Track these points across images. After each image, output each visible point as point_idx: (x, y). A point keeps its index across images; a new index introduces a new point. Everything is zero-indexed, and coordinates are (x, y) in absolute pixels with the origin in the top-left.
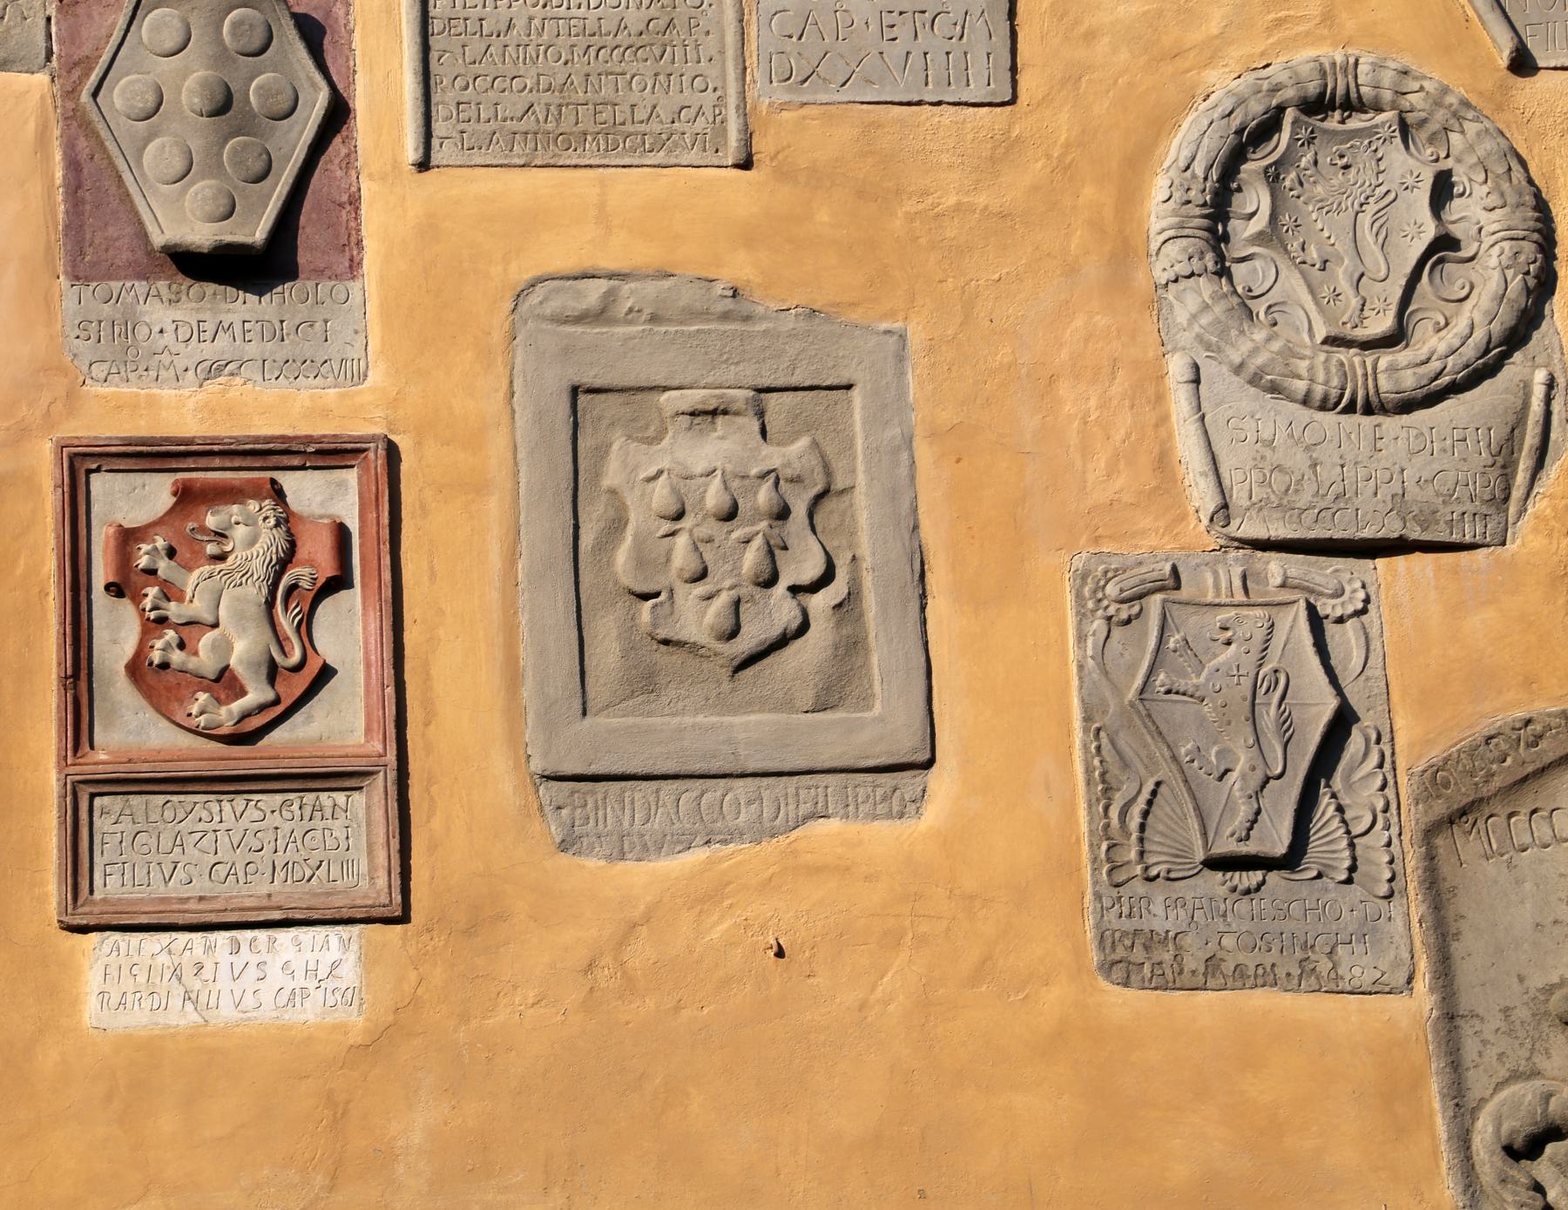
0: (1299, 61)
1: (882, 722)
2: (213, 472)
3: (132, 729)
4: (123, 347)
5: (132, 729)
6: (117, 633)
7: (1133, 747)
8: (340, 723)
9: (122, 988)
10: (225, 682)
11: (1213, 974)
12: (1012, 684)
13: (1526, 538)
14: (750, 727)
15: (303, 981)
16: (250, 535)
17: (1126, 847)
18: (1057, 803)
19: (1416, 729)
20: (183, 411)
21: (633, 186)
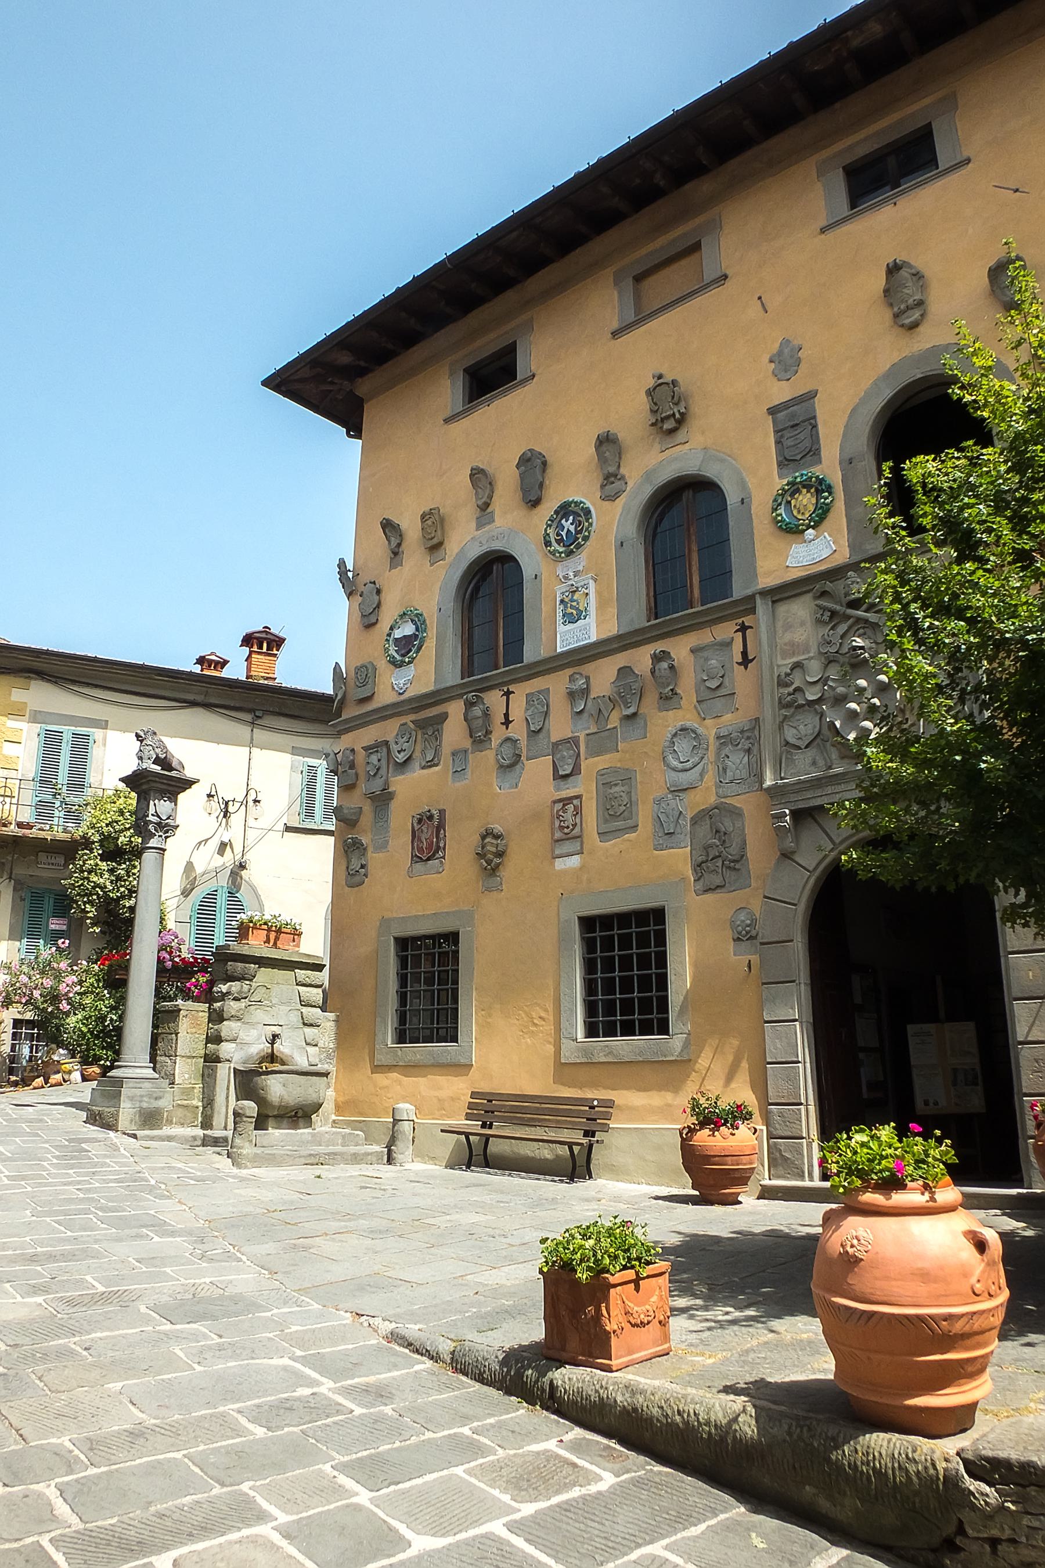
0: (679, 724)
1: (630, 823)
2: (566, 801)
3: (558, 835)
8: (577, 829)
9: (560, 864)
10: (568, 827)
11: (667, 848)
14: (620, 824)
15: (574, 861)
16: (570, 808)
20: (565, 794)
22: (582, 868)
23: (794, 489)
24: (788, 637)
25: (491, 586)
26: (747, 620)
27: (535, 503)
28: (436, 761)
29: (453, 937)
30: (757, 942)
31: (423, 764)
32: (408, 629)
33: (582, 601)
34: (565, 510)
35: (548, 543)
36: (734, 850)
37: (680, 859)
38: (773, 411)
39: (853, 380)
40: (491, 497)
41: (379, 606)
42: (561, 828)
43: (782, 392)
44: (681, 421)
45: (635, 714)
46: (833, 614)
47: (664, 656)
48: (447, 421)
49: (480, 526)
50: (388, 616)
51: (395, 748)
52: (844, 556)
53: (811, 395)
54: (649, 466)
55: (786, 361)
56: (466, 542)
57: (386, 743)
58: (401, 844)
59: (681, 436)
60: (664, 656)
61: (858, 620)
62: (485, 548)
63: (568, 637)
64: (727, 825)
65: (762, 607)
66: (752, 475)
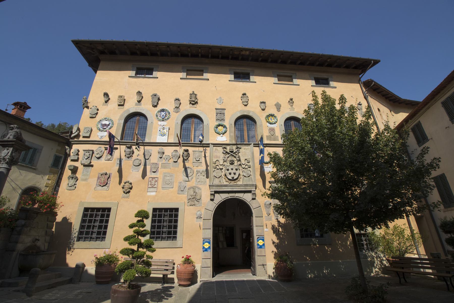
1: (171, 186)
3: (150, 186)
4: (151, 174)
5: (150, 186)
6: (150, 183)
7: (179, 187)
8: (155, 186)
12: (176, 186)
13: (192, 181)
14: (168, 186)
15: (154, 194)
16: (154, 180)
17: (178, 190)
18: (177, 189)
19: (188, 187)
20: (153, 176)
21: (167, 170)
22: (156, 196)
23: (219, 125)
24: (215, 154)
25: (135, 120)
26: (207, 148)
27: (155, 106)
28: (111, 159)
29: (109, 210)
30: (202, 219)
31: (106, 159)
32: (107, 123)
33: (161, 131)
34: (163, 110)
35: (157, 116)
36: (198, 197)
37: (184, 197)
38: (216, 109)
39: (234, 110)
40: (141, 100)
41: (97, 114)
42: (151, 184)
43: (219, 107)
44: (197, 103)
45: (176, 162)
46: (227, 152)
47: (187, 151)
48: (129, 77)
49: (136, 105)
50: (98, 118)
51: (95, 153)
52: (228, 142)
53: (225, 109)
54: (187, 109)
55: (220, 101)
56: (131, 106)
57: (93, 151)
58: (93, 181)
59: (195, 106)
60: (187, 151)
61: (231, 155)
62: (139, 111)
63: (160, 139)
64: (197, 190)
65: (211, 146)
66: (210, 120)
